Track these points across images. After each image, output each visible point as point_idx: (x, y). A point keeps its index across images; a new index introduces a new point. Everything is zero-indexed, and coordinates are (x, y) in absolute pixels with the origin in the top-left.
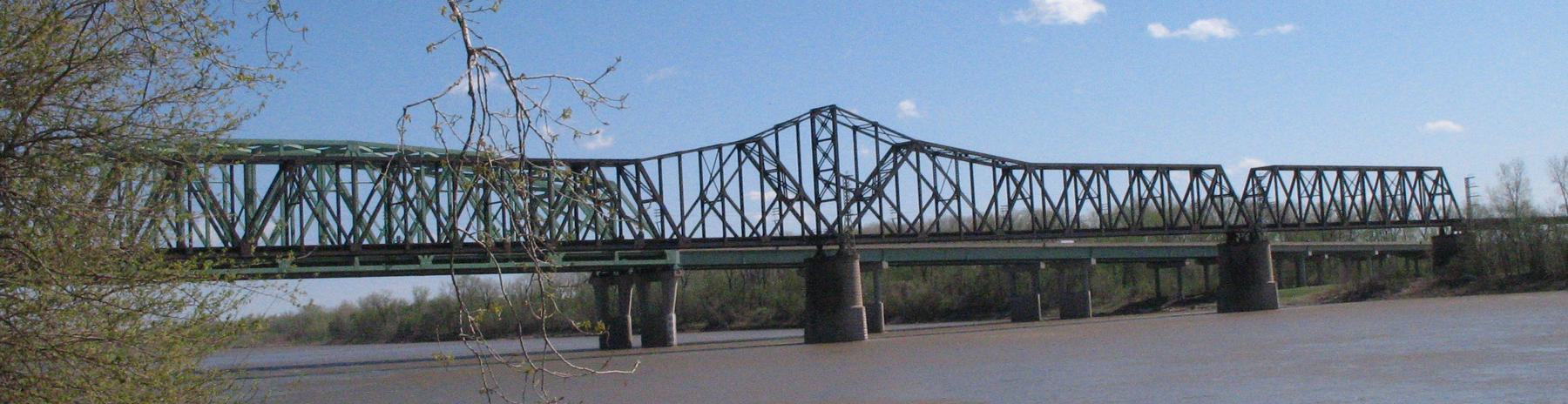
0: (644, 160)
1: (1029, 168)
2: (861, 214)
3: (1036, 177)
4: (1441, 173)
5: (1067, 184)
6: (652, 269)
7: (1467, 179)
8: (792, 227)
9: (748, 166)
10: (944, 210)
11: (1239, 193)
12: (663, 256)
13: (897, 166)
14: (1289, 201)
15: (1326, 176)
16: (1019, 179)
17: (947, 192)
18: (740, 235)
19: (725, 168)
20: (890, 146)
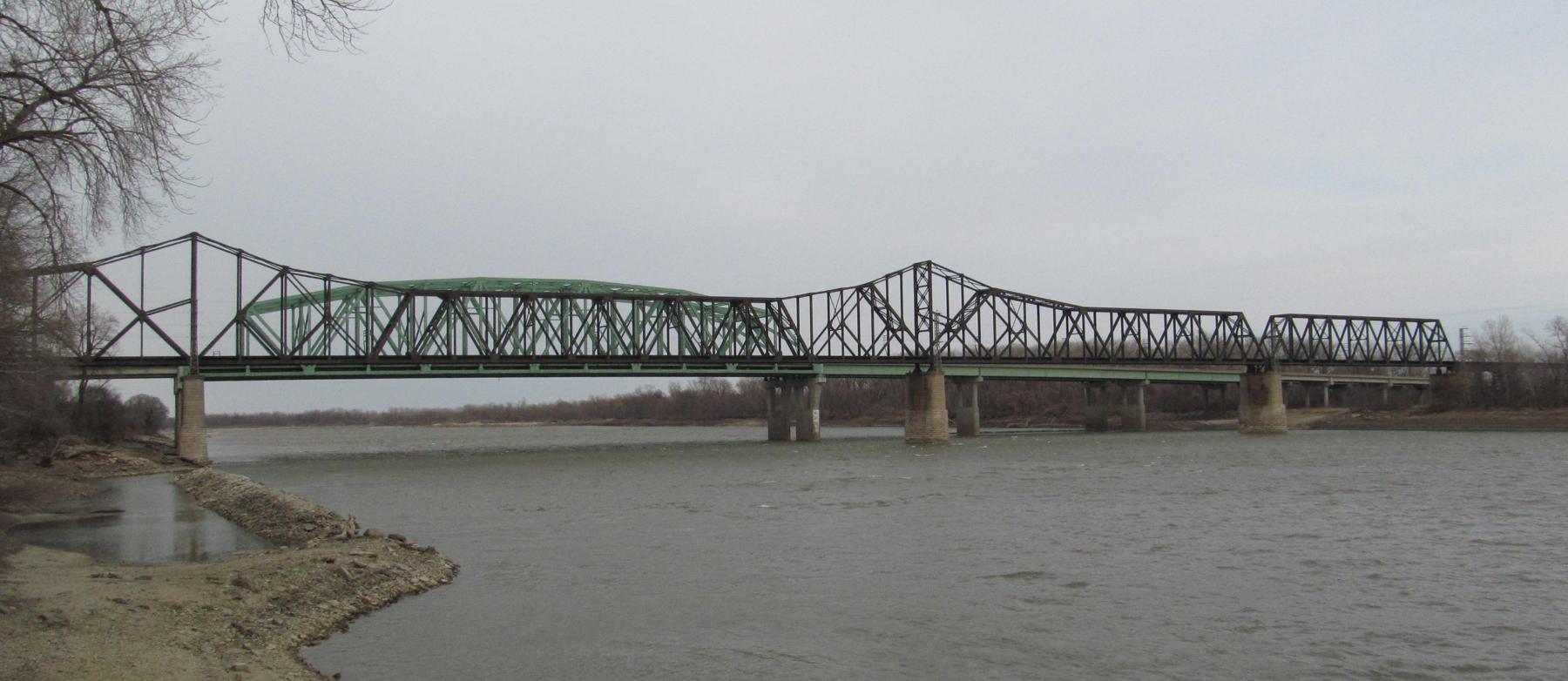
0: (784, 299)
1: (1083, 311)
2: (950, 339)
3: (1144, 321)
4: (1438, 324)
5: (1167, 326)
6: (806, 376)
7: (1461, 330)
8: (896, 350)
9: (864, 303)
10: (1014, 339)
11: (1258, 334)
12: (811, 368)
13: (979, 304)
14: (1413, 344)
15: (1373, 325)
16: (1183, 321)
17: (1017, 327)
18: (857, 354)
19: (845, 308)
20: (974, 292)
